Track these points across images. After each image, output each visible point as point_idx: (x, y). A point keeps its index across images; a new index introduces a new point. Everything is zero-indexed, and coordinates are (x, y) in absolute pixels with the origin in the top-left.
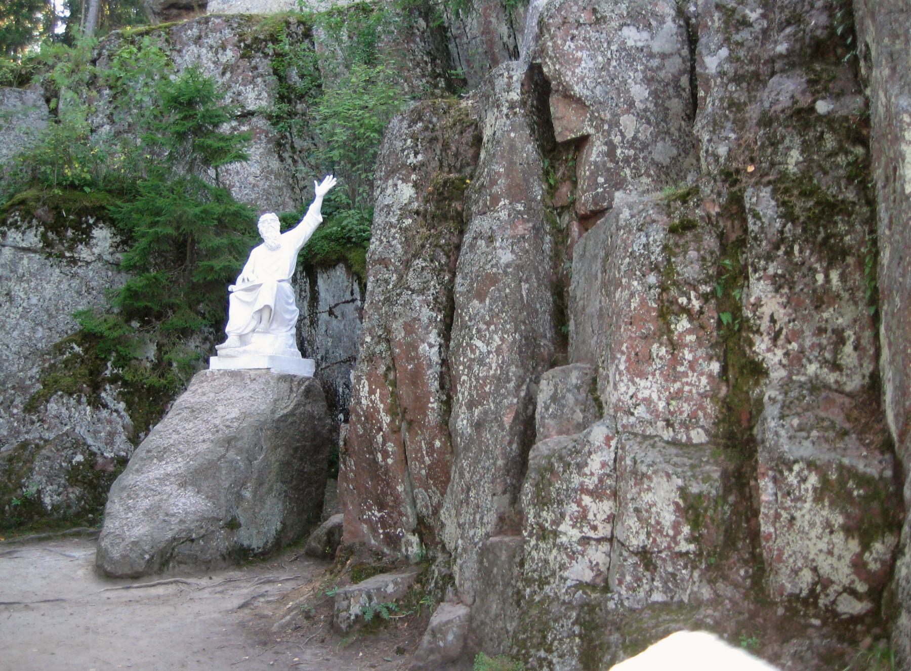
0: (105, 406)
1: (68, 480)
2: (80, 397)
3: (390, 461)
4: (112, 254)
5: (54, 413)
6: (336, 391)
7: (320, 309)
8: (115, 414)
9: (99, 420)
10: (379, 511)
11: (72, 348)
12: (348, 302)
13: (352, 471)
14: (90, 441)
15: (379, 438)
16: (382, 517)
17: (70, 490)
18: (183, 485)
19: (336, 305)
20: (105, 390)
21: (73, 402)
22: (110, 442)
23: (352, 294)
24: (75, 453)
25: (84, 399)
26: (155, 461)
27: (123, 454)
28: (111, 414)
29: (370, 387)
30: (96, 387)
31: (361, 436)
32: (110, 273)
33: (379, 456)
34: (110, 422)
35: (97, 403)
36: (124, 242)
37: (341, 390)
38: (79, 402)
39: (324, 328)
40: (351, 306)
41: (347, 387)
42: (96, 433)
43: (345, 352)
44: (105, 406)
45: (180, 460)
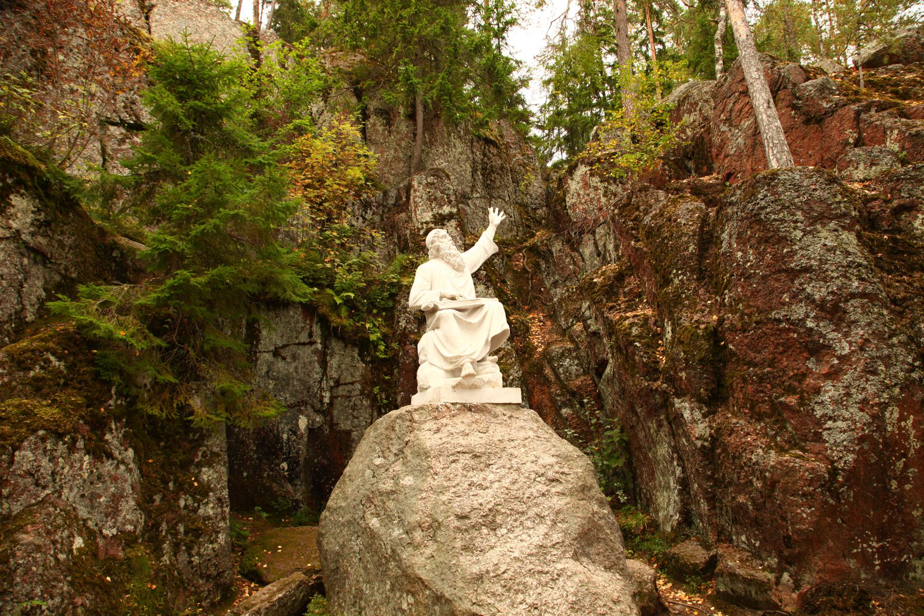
0: (110, 456)
1: (71, 584)
2: (74, 440)
3: (908, 487)
4: (33, 234)
5: (26, 467)
6: (278, 438)
7: (261, 347)
8: (122, 467)
9: (100, 477)
10: (877, 542)
11: (48, 361)
12: (304, 344)
13: (847, 502)
14: (83, 512)
15: (900, 464)
16: (882, 547)
17: (78, 600)
18: (576, 557)
19: (284, 346)
20: (111, 430)
21: (62, 448)
22: (113, 511)
23: (311, 335)
24: (71, 536)
25: (80, 444)
26: (485, 531)
27: (129, 528)
28: (117, 467)
29: (901, 414)
30: (99, 425)
31: (871, 465)
32: (26, 261)
33: (894, 484)
34: (115, 479)
35: (99, 452)
36: (47, 224)
37: (285, 436)
38: (72, 448)
39: (265, 369)
40: (308, 350)
41: (295, 433)
42: (94, 497)
43: (292, 395)
44: (110, 456)
45: (529, 524)
